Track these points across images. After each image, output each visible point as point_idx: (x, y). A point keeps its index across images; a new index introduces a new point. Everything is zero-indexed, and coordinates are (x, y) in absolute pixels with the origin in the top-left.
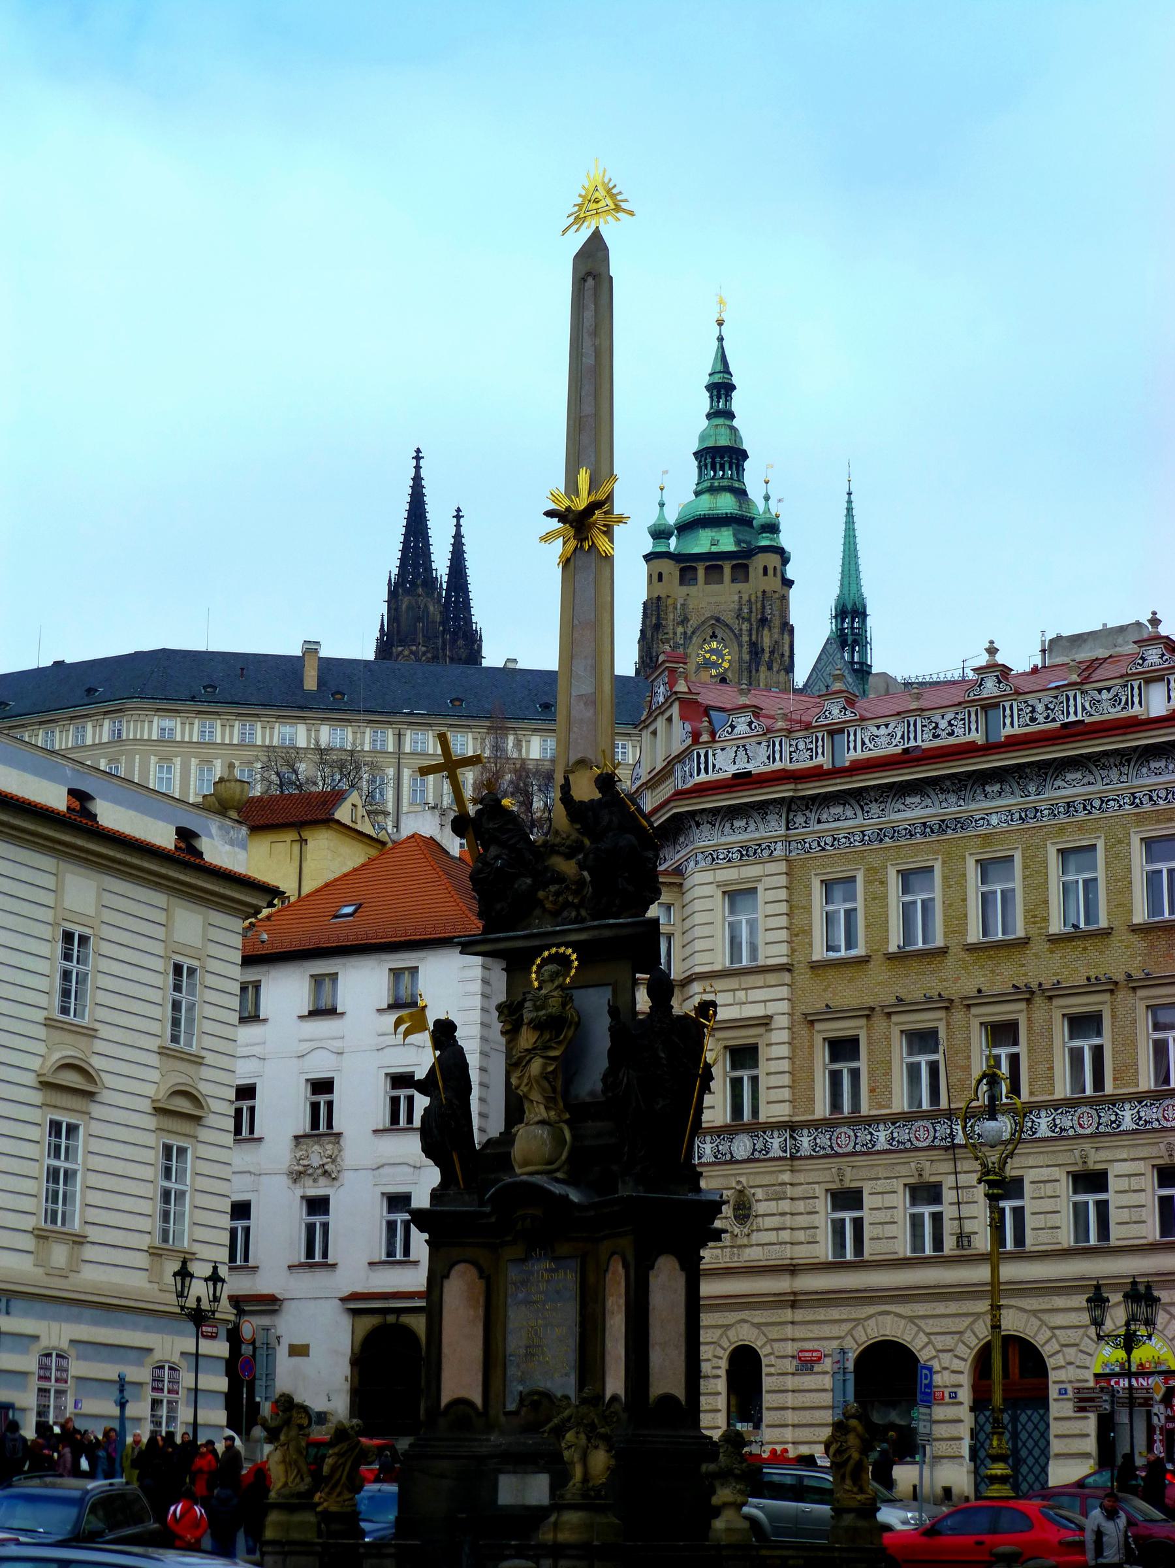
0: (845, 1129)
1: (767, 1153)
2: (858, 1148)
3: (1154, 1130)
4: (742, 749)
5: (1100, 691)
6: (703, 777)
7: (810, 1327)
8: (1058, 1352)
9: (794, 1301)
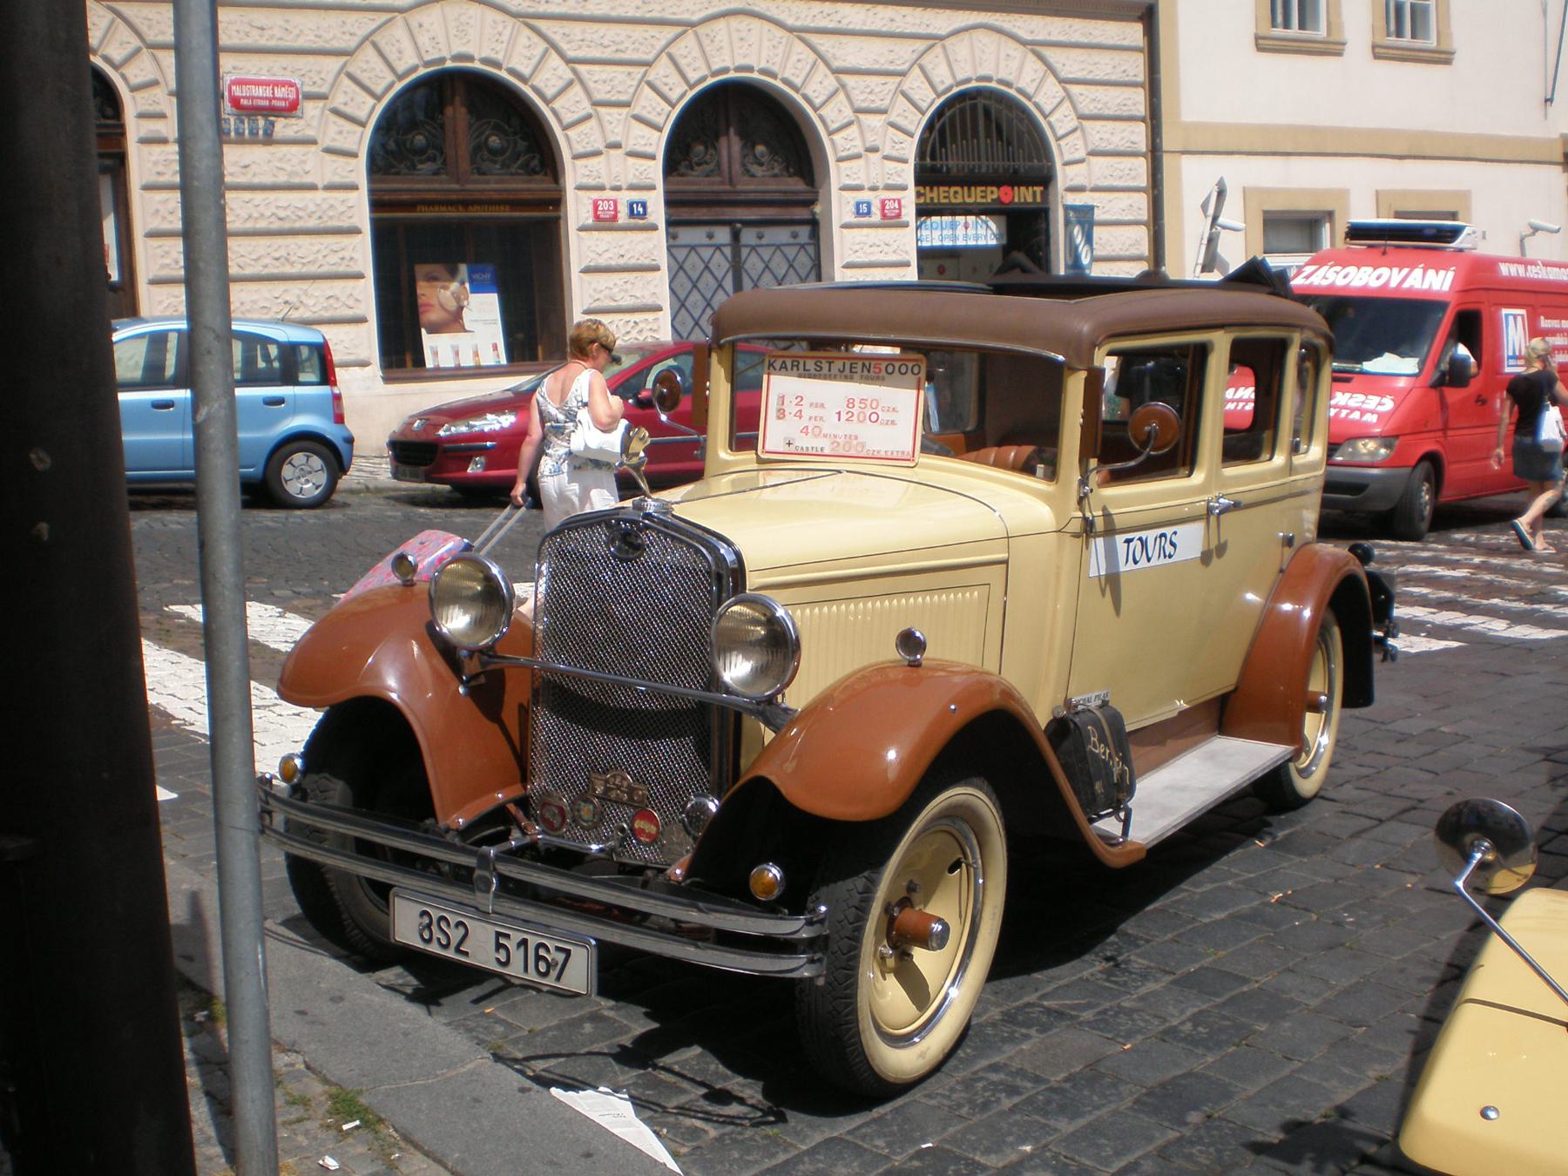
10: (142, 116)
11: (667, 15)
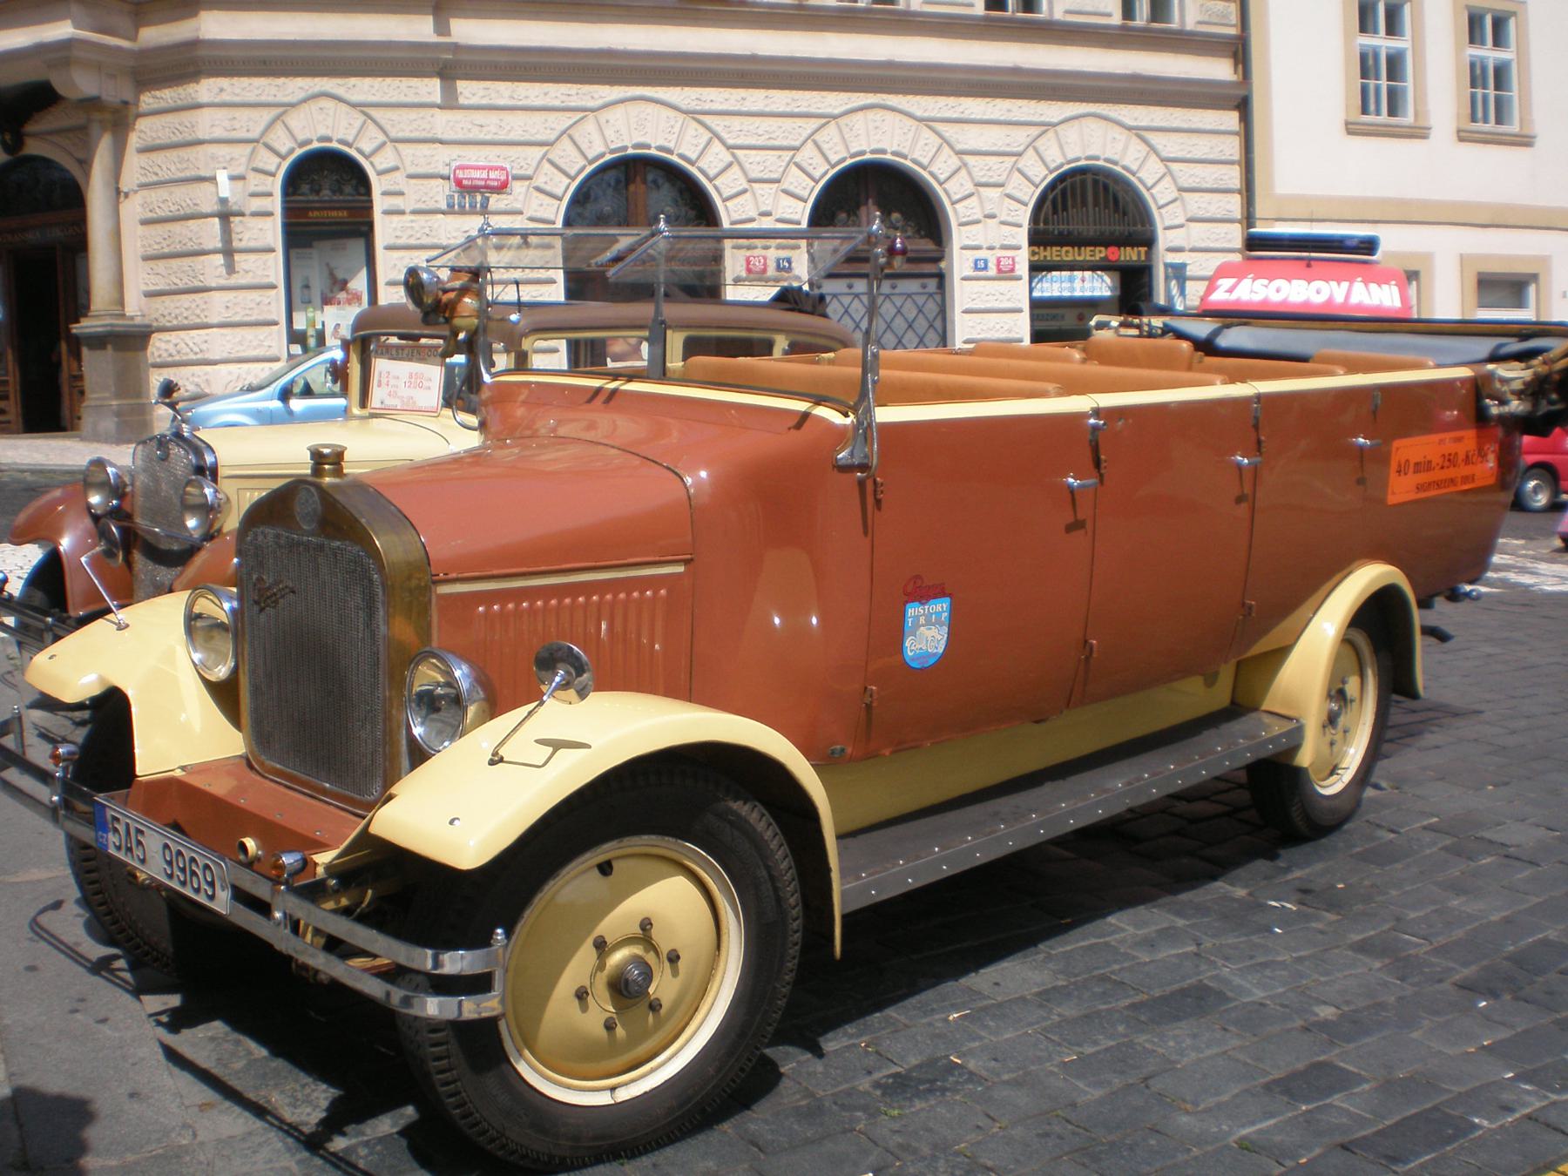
8: (971, 195)
10: (385, 193)
11: (812, 110)
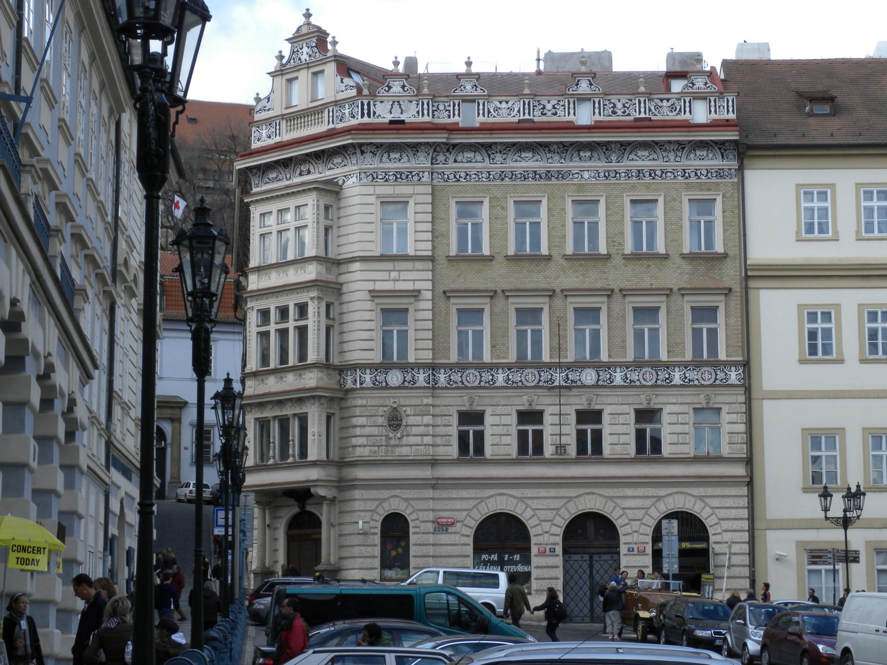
0: (473, 371)
1: (415, 383)
2: (482, 384)
3: (695, 386)
4: (396, 104)
5: (662, 100)
6: (366, 119)
7: (446, 502)
9: (436, 484)
10: (414, 527)
